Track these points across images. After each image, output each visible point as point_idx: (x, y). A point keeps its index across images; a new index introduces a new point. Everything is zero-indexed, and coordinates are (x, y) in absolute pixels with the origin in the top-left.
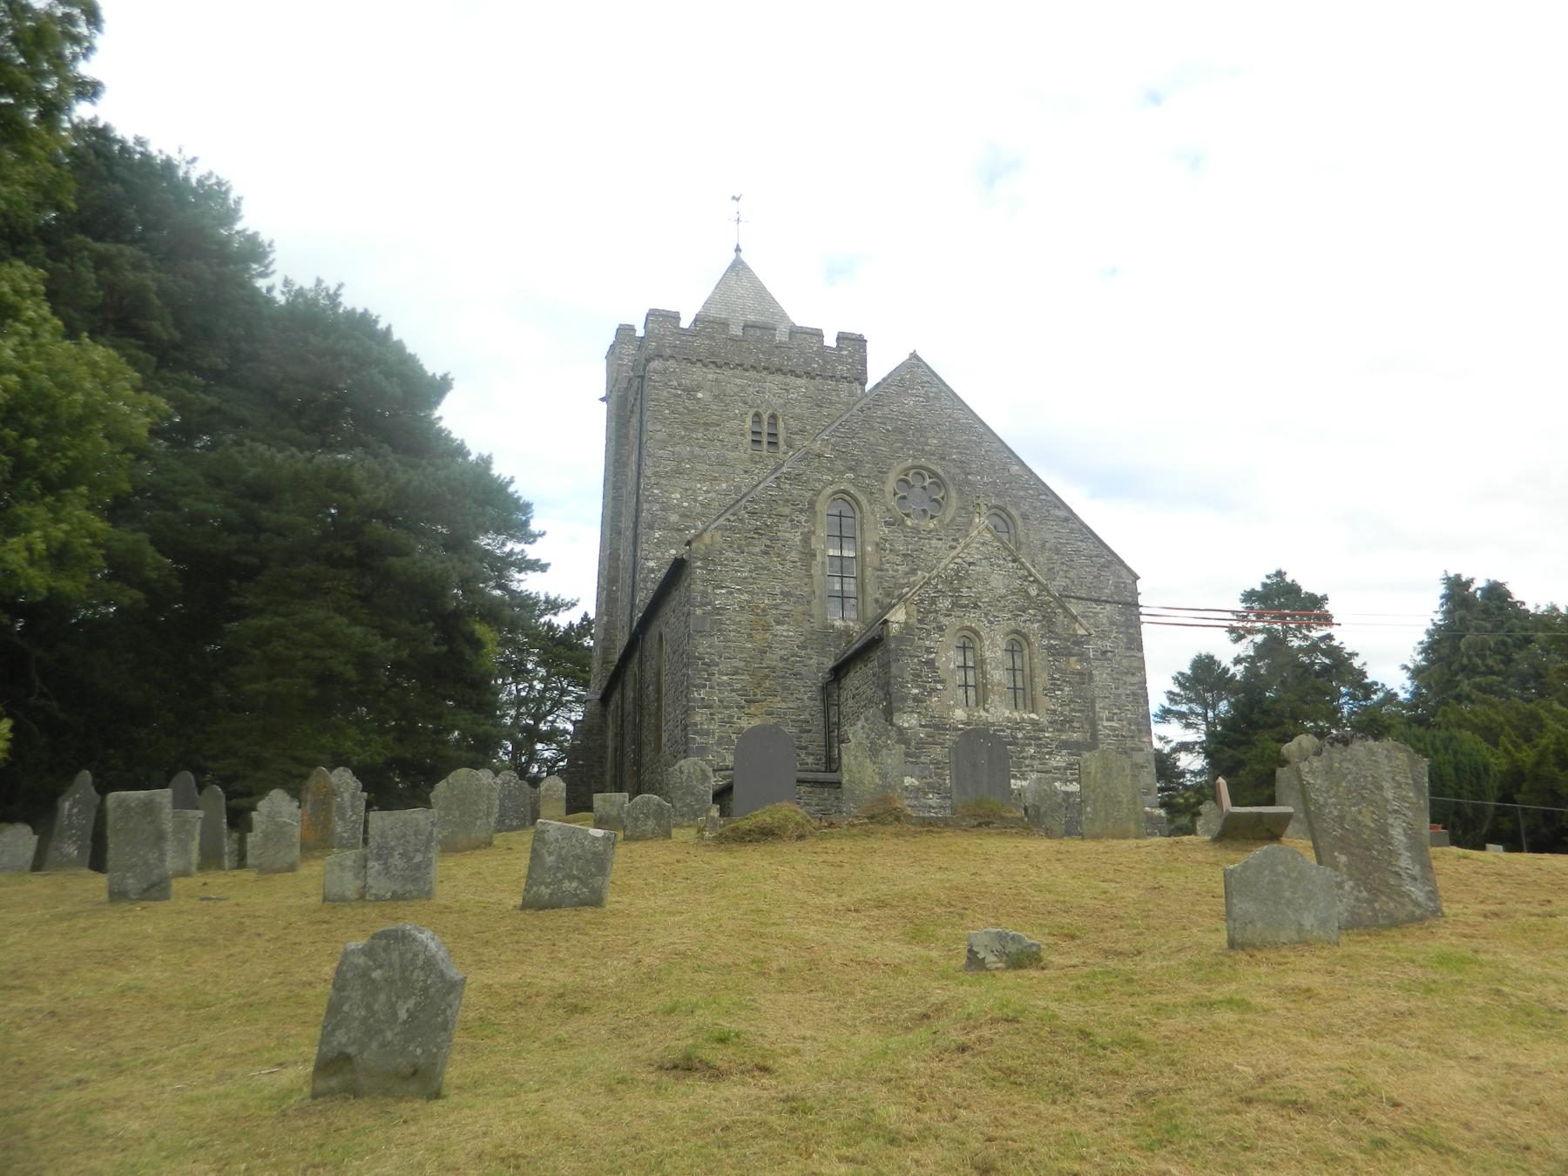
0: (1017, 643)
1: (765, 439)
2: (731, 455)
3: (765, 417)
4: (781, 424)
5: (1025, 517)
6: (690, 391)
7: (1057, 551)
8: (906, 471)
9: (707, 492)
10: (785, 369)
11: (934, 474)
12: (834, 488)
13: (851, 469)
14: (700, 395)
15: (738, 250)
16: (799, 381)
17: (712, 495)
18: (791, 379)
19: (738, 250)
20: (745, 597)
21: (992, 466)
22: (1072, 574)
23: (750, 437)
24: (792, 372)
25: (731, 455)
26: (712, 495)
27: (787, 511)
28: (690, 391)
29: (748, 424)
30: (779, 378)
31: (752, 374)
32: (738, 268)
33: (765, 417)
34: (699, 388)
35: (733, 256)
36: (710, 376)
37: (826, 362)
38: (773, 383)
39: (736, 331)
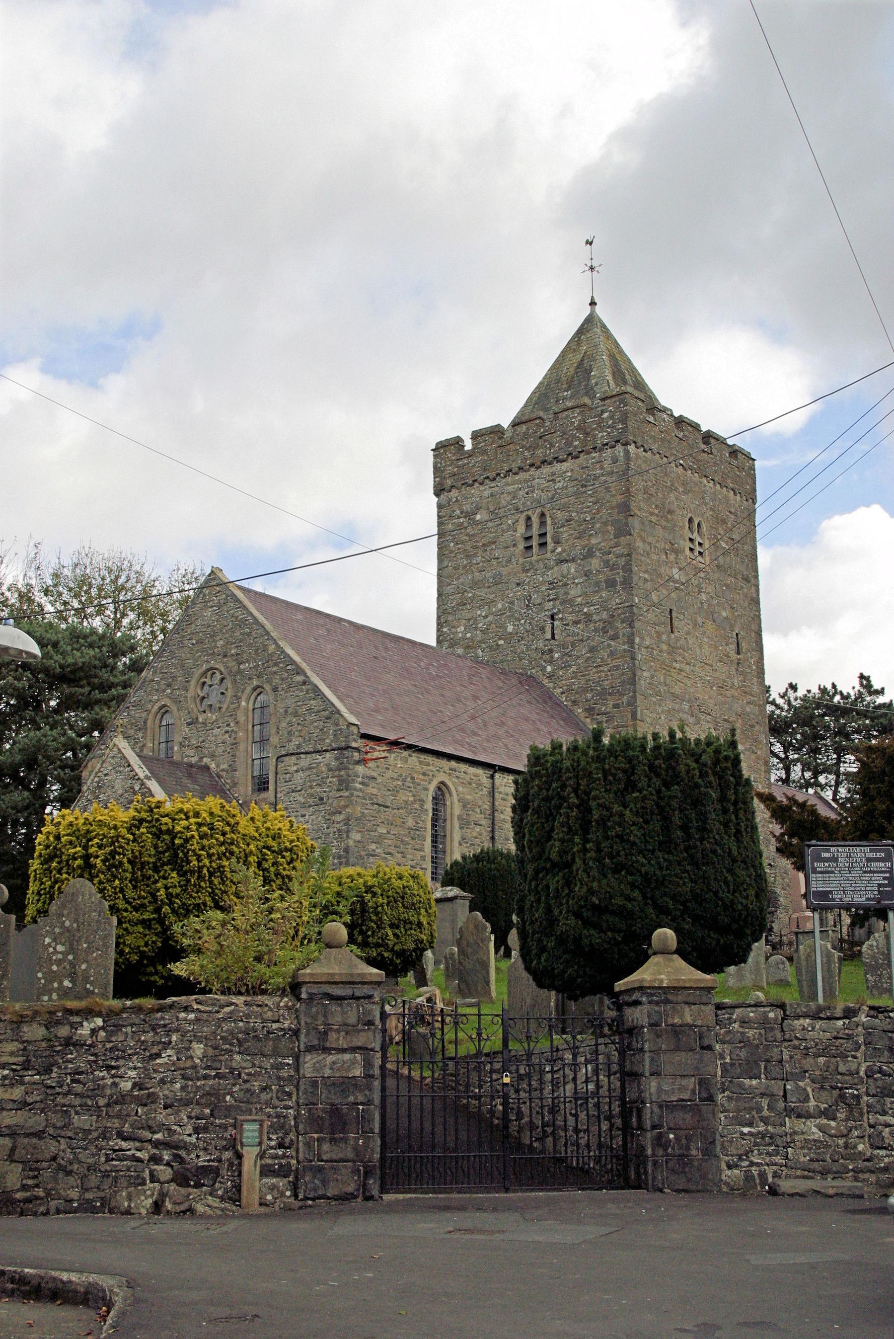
1: (535, 543)
2: (504, 571)
3: (535, 519)
6: (468, 515)
9: (486, 617)
13: (169, 685)
15: (593, 303)
16: (565, 466)
17: (490, 618)
18: (558, 467)
19: (593, 303)
23: (521, 545)
25: (504, 571)
29: (521, 529)
30: (546, 470)
31: (522, 476)
32: (590, 325)
33: (535, 519)
34: (478, 509)
35: (587, 311)
37: (587, 434)
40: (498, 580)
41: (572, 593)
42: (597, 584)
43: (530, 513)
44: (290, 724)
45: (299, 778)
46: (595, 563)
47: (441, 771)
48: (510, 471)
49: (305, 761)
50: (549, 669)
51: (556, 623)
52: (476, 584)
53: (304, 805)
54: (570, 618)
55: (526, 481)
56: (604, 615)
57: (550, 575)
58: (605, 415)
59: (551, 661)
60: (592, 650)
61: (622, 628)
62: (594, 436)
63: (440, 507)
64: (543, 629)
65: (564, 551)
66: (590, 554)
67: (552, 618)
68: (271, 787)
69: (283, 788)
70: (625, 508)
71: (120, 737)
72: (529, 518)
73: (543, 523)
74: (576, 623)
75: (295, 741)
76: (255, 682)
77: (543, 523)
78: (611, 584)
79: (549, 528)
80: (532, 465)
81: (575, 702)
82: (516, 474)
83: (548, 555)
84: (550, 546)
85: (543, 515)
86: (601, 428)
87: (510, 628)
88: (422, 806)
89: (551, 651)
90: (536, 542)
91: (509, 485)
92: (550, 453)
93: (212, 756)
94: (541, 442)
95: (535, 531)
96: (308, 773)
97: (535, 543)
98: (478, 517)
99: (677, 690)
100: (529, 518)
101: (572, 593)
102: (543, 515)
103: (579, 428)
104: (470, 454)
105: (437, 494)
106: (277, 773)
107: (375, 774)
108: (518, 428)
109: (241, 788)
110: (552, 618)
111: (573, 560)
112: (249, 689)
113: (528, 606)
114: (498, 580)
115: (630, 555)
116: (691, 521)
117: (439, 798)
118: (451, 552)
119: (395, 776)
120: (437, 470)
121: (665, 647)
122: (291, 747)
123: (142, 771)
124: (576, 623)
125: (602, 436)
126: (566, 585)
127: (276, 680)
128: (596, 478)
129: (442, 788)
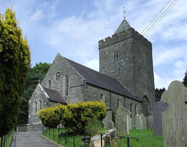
1: (116, 56)
2: (111, 62)
3: (116, 52)
5: (69, 75)
6: (105, 53)
10: (118, 41)
15: (125, 17)
19: (125, 17)
28: (105, 53)
29: (114, 54)
30: (118, 43)
33: (116, 52)
34: (106, 51)
38: (117, 45)
41: (123, 64)
44: (72, 81)
45: (74, 92)
46: (127, 59)
47: (102, 91)
49: (75, 88)
50: (119, 78)
53: (75, 97)
55: (114, 46)
56: (129, 68)
59: (119, 77)
60: (126, 74)
65: (121, 57)
66: (126, 57)
67: (119, 69)
68: (69, 94)
71: (39, 84)
72: (115, 52)
73: (118, 53)
74: (123, 70)
75: (73, 84)
76: (66, 74)
77: (118, 53)
79: (119, 54)
81: (124, 84)
82: (113, 45)
85: (117, 51)
88: (98, 98)
89: (119, 75)
90: (116, 56)
91: (112, 47)
92: (119, 40)
93: (58, 89)
95: (116, 54)
97: (116, 56)
99: (141, 81)
100: (115, 52)
101: (123, 64)
102: (117, 51)
104: (105, 42)
105: (99, 50)
107: (89, 91)
109: (63, 94)
110: (119, 69)
116: (142, 52)
117: (102, 94)
119: (93, 91)
121: (139, 74)
122: (72, 86)
123: (43, 90)
124: (123, 70)
125: (128, 36)
126: (121, 63)
127: (70, 73)
128: (127, 44)
129: (102, 94)
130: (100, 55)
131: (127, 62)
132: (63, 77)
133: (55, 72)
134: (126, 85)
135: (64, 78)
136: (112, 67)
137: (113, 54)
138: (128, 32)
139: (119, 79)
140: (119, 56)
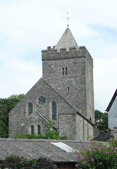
0: (39, 127)
1: (65, 73)
3: (65, 69)
4: (68, 69)
5: (58, 102)
7: (63, 107)
8: (40, 97)
9: (54, 86)
10: (68, 57)
11: (44, 97)
12: (29, 102)
13: (31, 99)
14: (52, 66)
15: (68, 26)
17: (55, 86)
19: (68, 26)
20: (16, 120)
21: (53, 95)
22: (65, 110)
23: (62, 73)
24: (70, 58)
25: (58, 78)
26: (55, 86)
27: (22, 107)
28: (50, 66)
32: (67, 30)
33: (65, 69)
34: (52, 65)
36: (54, 62)
38: (66, 61)
39: (59, 51)
40: (56, 79)
42: (78, 83)
43: (64, 67)
45: (64, 118)
46: (78, 79)
48: (59, 58)
49: (65, 116)
50: (68, 97)
51: (69, 89)
52: (51, 79)
54: (72, 88)
56: (80, 89)
57: (68, 80)
58: (81, 51)
61: (84, 92)
62: (78, 55)
63: (43, 63)
64: (66, 90)
66: (76, 77)
69: (60, 120)
70: (84, 70)
75: (63, 112)
78: (81, 83)
80: (64, 58)
81: (73, 104)
82: (61, 59)
83: (68, 76)
84: (68, 74)
86: (79, 53)
87: (59, 89)
91: (59, 62)
92: (69, 56)
94: (67, 54)
96: (66, 118)
97: (65, 73)
98: (52, 66)
101: (73, 84)
103: (75, 53)
105: (42, 61)
106: (58, 117)
108: (61, 51)
111: (73, 77)
112: (51, 101)
113: (63, 85)
114: (56, 79)
115: (85, 78)
118: (46, 72)
120: (42, 56)
122: (62, 113)
127: (58, 100)
128: (78, 63)
130: (43, 67)
131: (78, 83)
132: (49, 103)
133: (38, 96)
134: (77, 106)
135: (51, 104)
136: (59, 84)
137: (60, 70)
138: (80, 50)
139: (68, 99)
140: (68, 73)
